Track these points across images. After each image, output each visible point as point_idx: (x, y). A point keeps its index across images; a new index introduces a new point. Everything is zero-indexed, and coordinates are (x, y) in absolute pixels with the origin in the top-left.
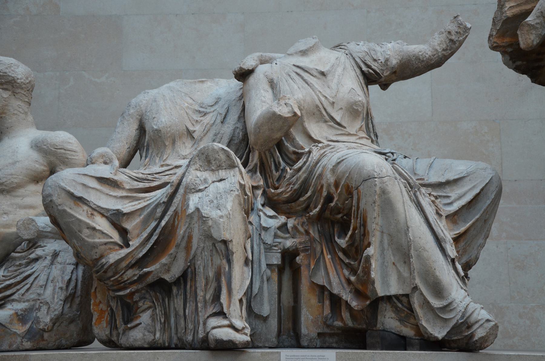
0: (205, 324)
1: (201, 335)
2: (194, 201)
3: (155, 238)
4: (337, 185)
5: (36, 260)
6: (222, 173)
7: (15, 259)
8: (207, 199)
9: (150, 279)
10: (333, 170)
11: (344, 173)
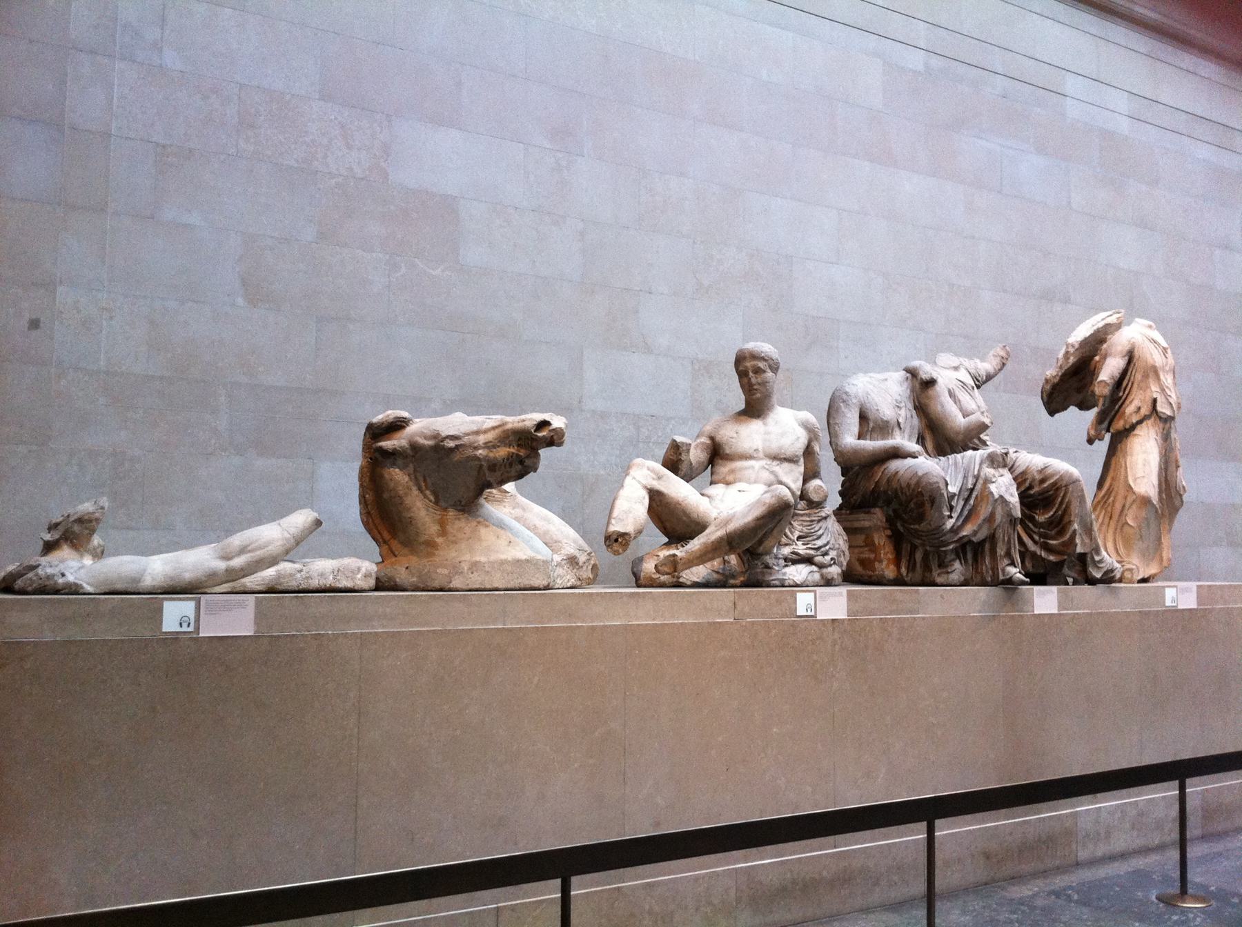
0: (1003, 570)
1: (1001, 577)
2: (993, 488)
3: (966, 513)
4: (1042, 481)
5: (825, 518)
6: (1001, 470)
7: (795, 515)
8: (1003, 489)
9: (965, 540)
10: (1041, 471)
11: (1053, 475)
